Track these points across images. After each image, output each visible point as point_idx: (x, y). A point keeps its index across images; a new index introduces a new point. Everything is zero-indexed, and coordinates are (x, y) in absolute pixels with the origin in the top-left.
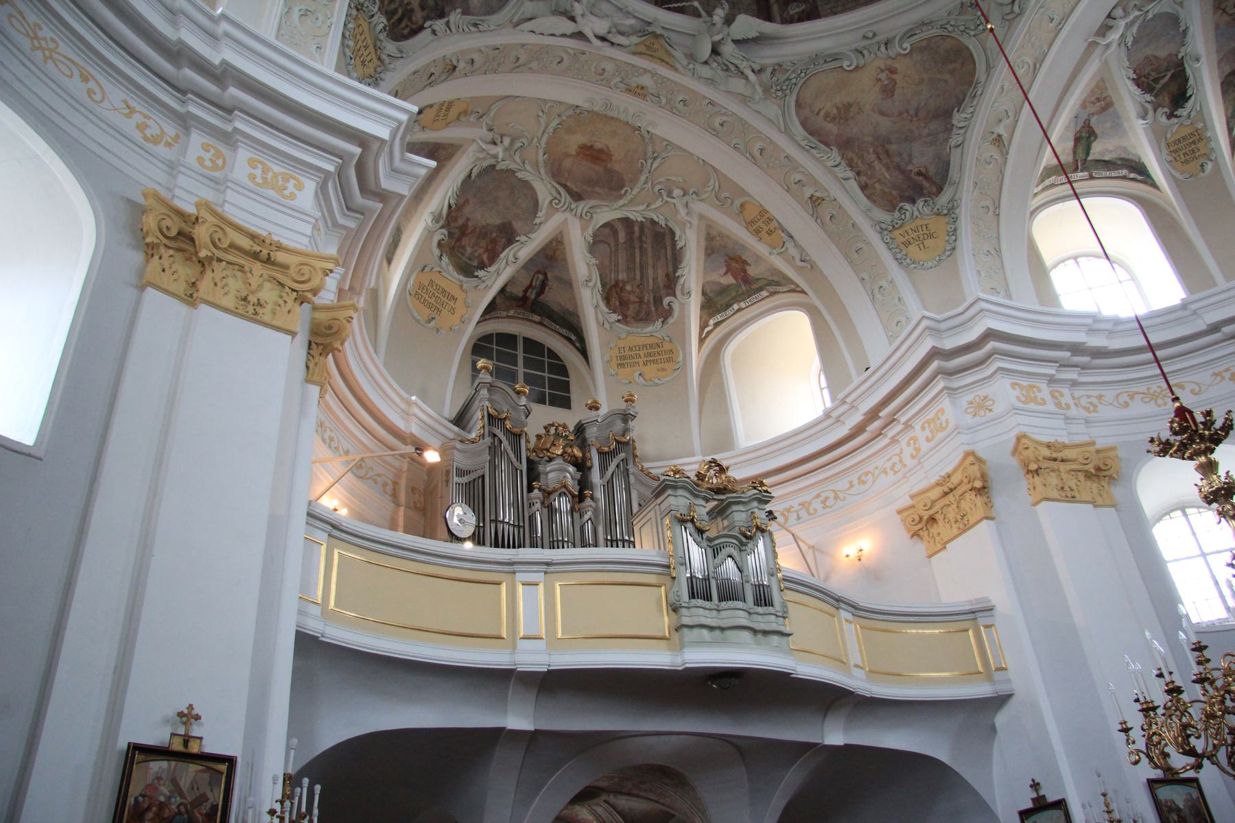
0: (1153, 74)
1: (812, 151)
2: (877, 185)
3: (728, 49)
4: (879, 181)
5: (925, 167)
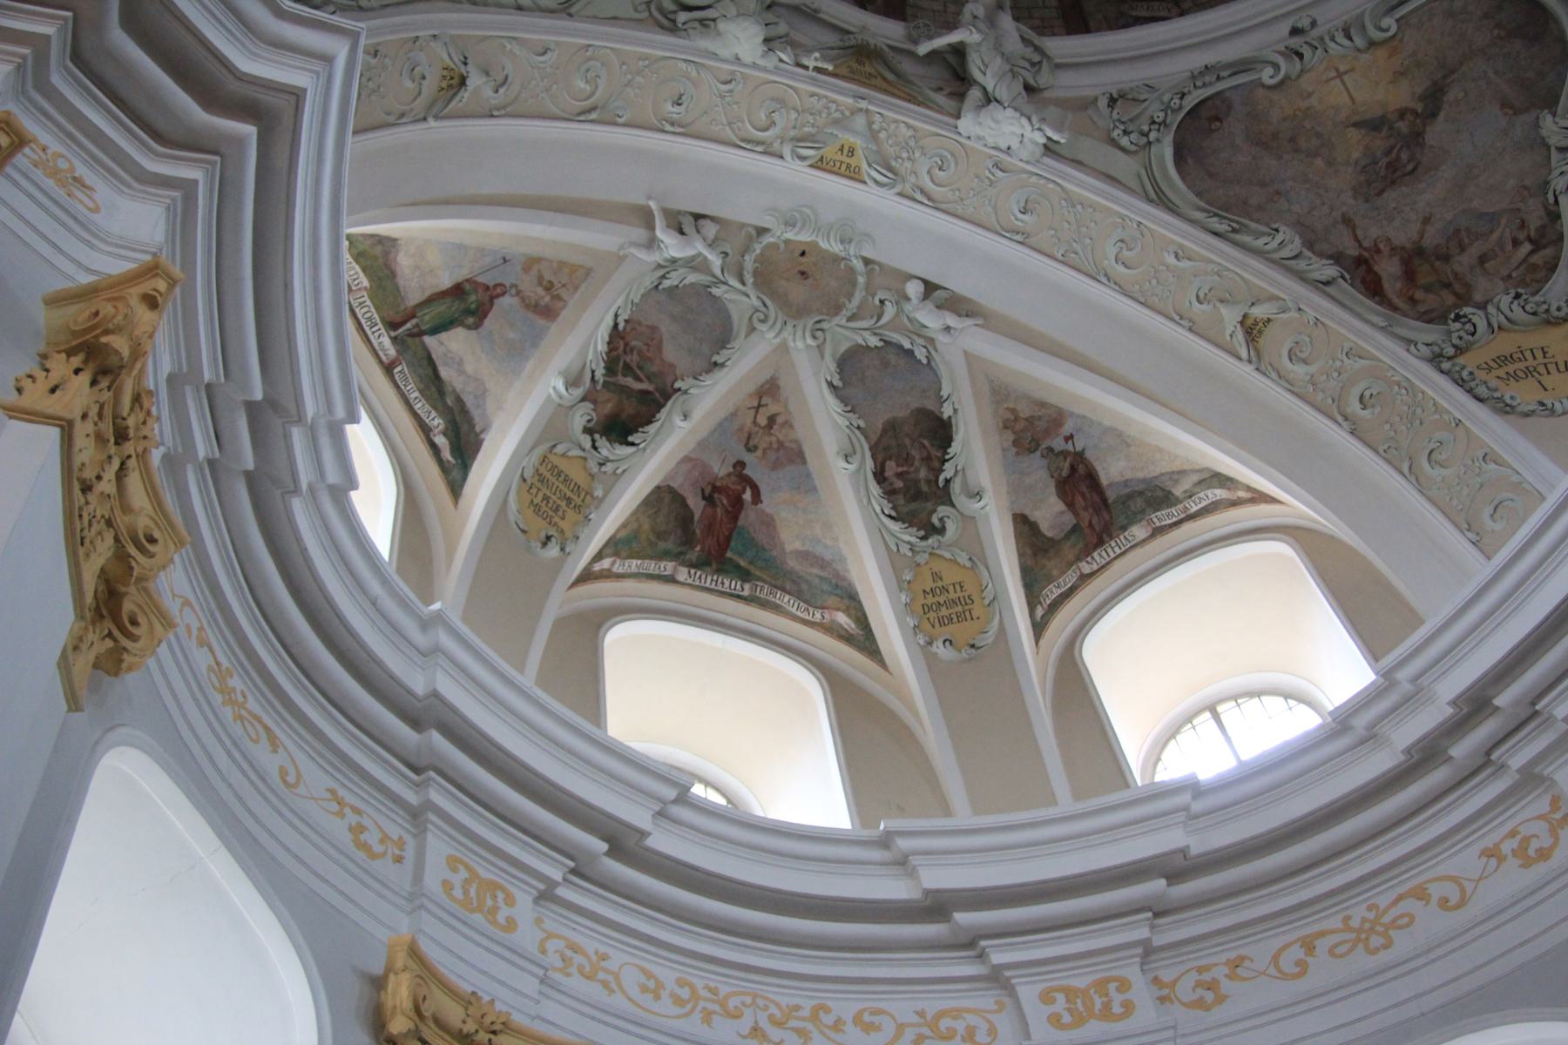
0: (635, 357)
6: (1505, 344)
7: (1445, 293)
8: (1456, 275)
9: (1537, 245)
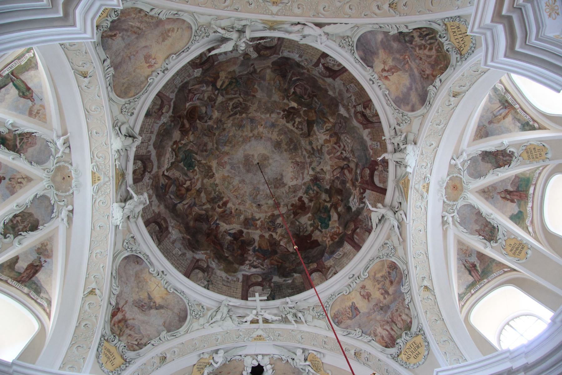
0: (26, 141)
1: (176, 12)
2: (133, 16)
3: (234, 35)
4: (134, 18)
5: (114, 40)
6: (113, 350)
7: (119, 331)
8: (124, 331)
9: (138, 345)
